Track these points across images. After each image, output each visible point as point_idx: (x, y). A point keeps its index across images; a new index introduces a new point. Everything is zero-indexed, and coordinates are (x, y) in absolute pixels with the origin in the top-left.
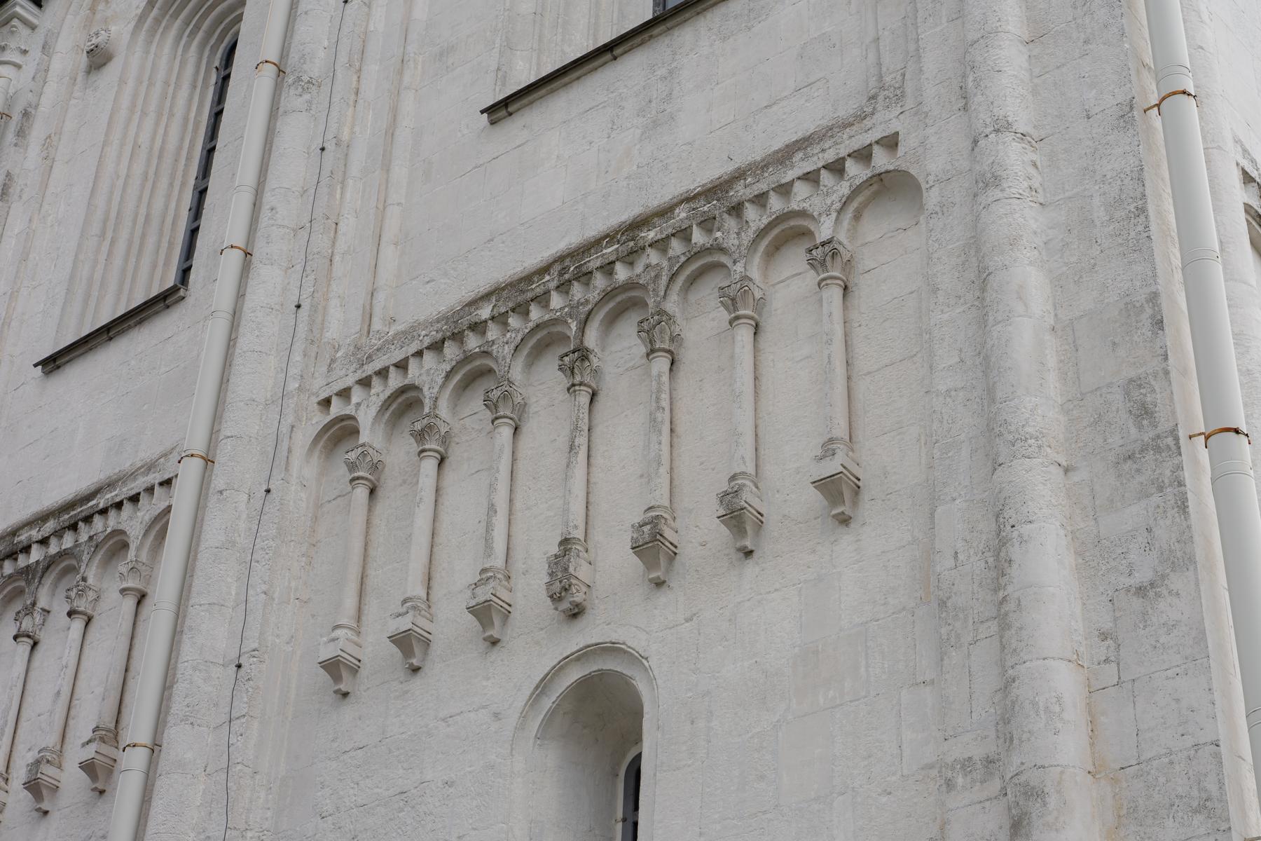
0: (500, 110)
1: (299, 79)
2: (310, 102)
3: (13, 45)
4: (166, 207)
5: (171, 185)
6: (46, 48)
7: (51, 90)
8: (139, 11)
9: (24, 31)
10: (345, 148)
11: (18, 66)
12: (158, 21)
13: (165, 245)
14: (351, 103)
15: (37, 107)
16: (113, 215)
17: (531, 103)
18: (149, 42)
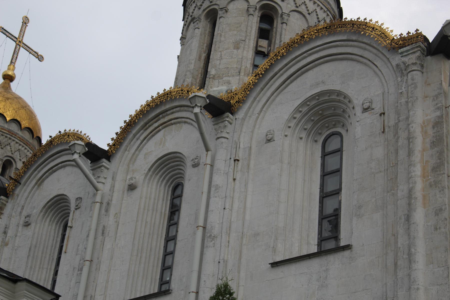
0: (275, 265)
1: (211, 236)
2: (214, 244)
3: (102, 176)
4: (156, 245)
5: (157, 237)
6: (113, 179)
7: (115, 194)
8: (146, 172)
9: (106, 170)
10: (225, 262)
11: (104, 183)
12: (151, 176)
13: (156, 259)
14: (227, 246)
15: (112, 200)
16: (140, 248)
17: (284, 264)
18: (148, 183)
